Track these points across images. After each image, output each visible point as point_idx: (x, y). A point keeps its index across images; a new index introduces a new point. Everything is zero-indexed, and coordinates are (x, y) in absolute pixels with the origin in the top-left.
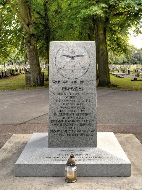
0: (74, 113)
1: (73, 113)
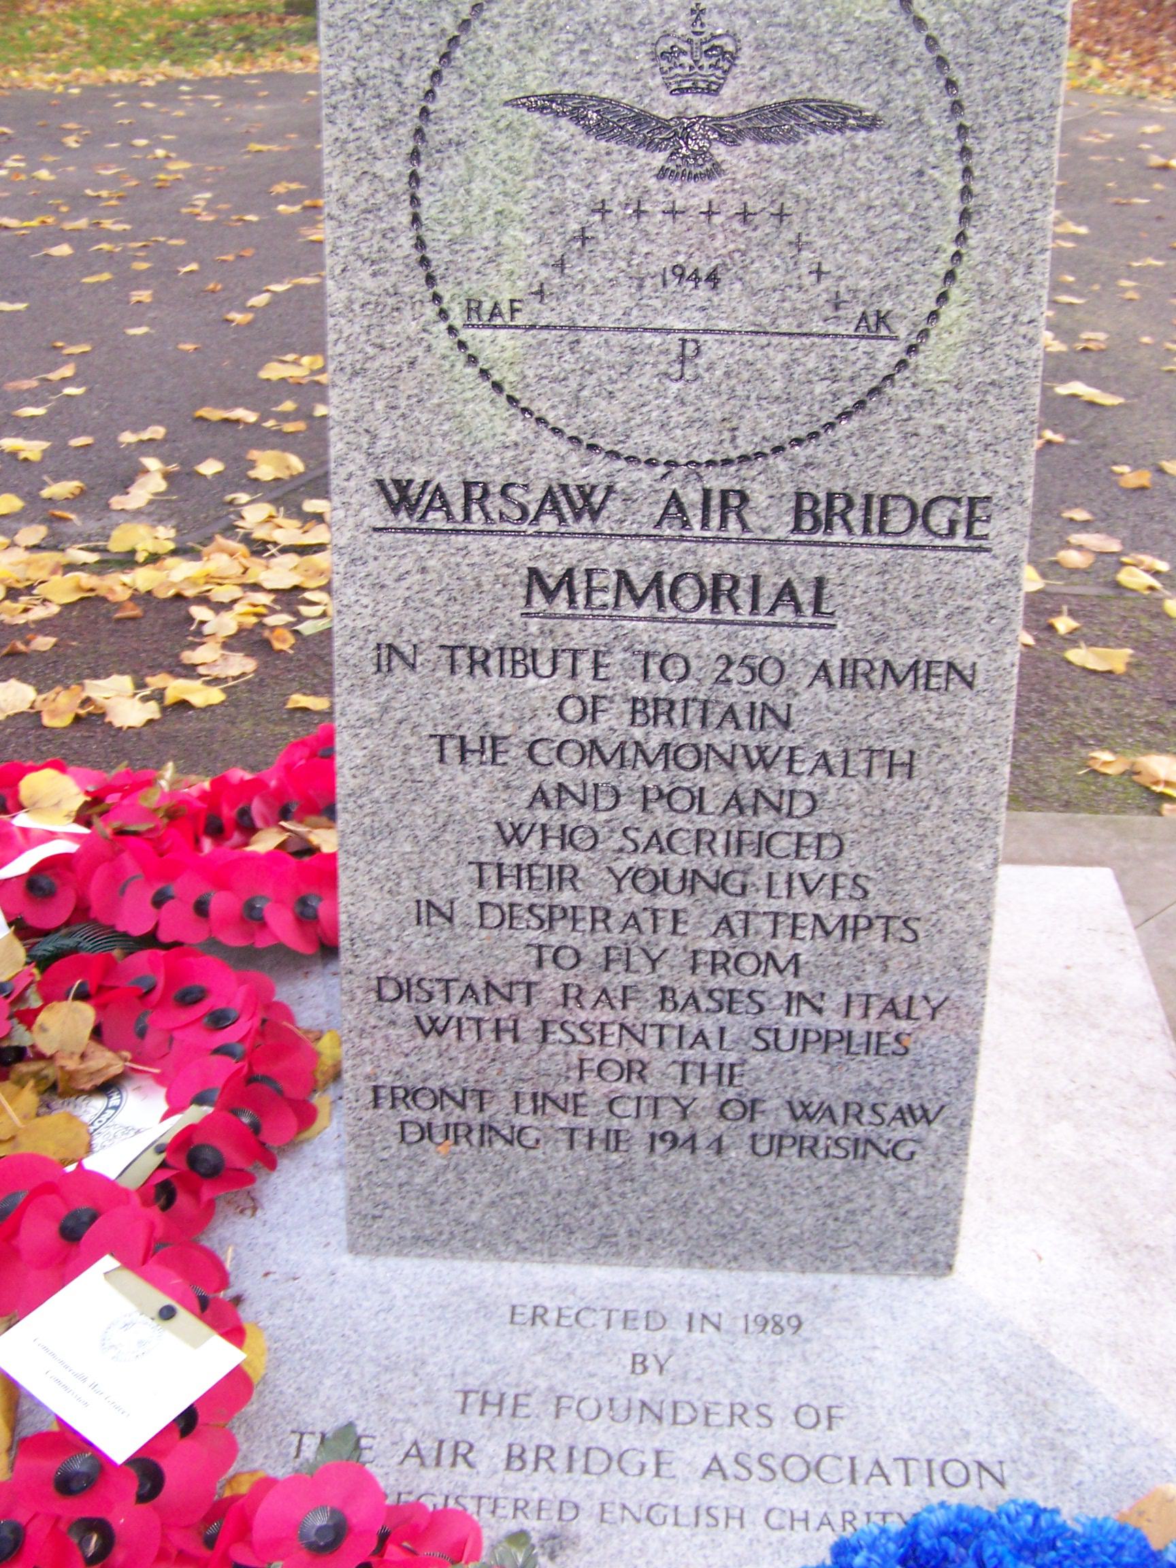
0: (682, 902)
1: (664, 901)
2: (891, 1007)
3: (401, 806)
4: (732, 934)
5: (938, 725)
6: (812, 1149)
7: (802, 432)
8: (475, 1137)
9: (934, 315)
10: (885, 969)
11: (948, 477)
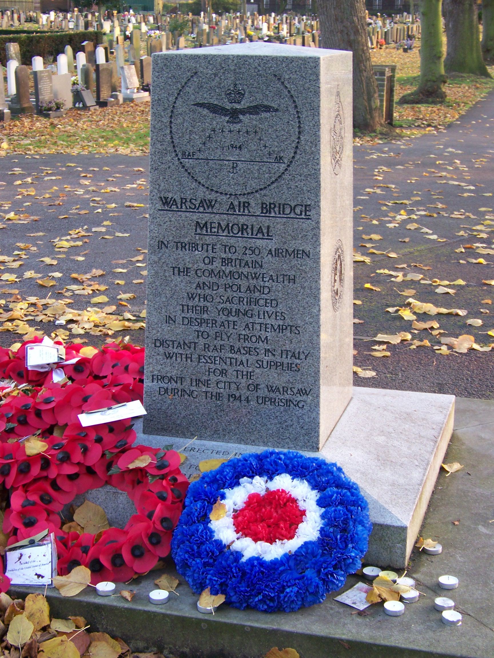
0: (235, 319)
1: (231, 318)
2: (293, 355)
3: (163, 287)
4: (249, 330)
5: (301, 268)
6: (274, 402)
7: (262, 187)
8: (180, 393)
9: (293, 157)
10: (291, 343)
11: (299, 199)
